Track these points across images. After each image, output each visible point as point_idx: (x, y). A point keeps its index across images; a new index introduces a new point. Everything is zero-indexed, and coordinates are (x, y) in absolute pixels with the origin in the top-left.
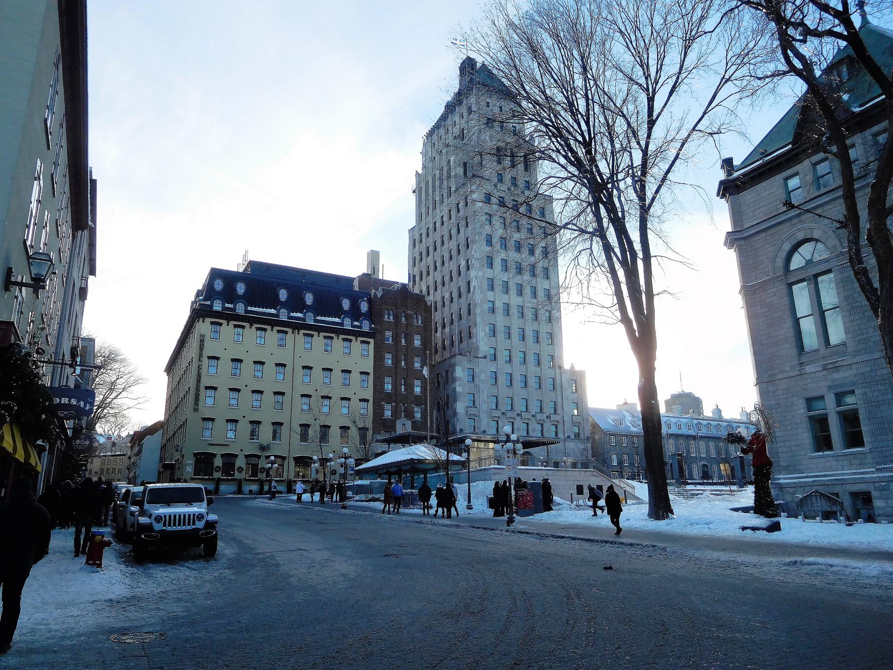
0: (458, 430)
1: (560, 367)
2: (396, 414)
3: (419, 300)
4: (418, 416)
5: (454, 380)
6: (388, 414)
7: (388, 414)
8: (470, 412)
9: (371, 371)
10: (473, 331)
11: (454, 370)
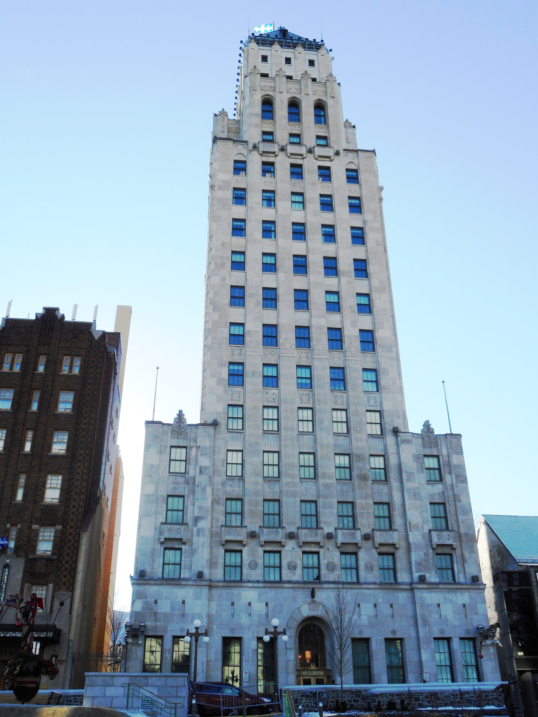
4: (45, 547)
8: (167, 535)
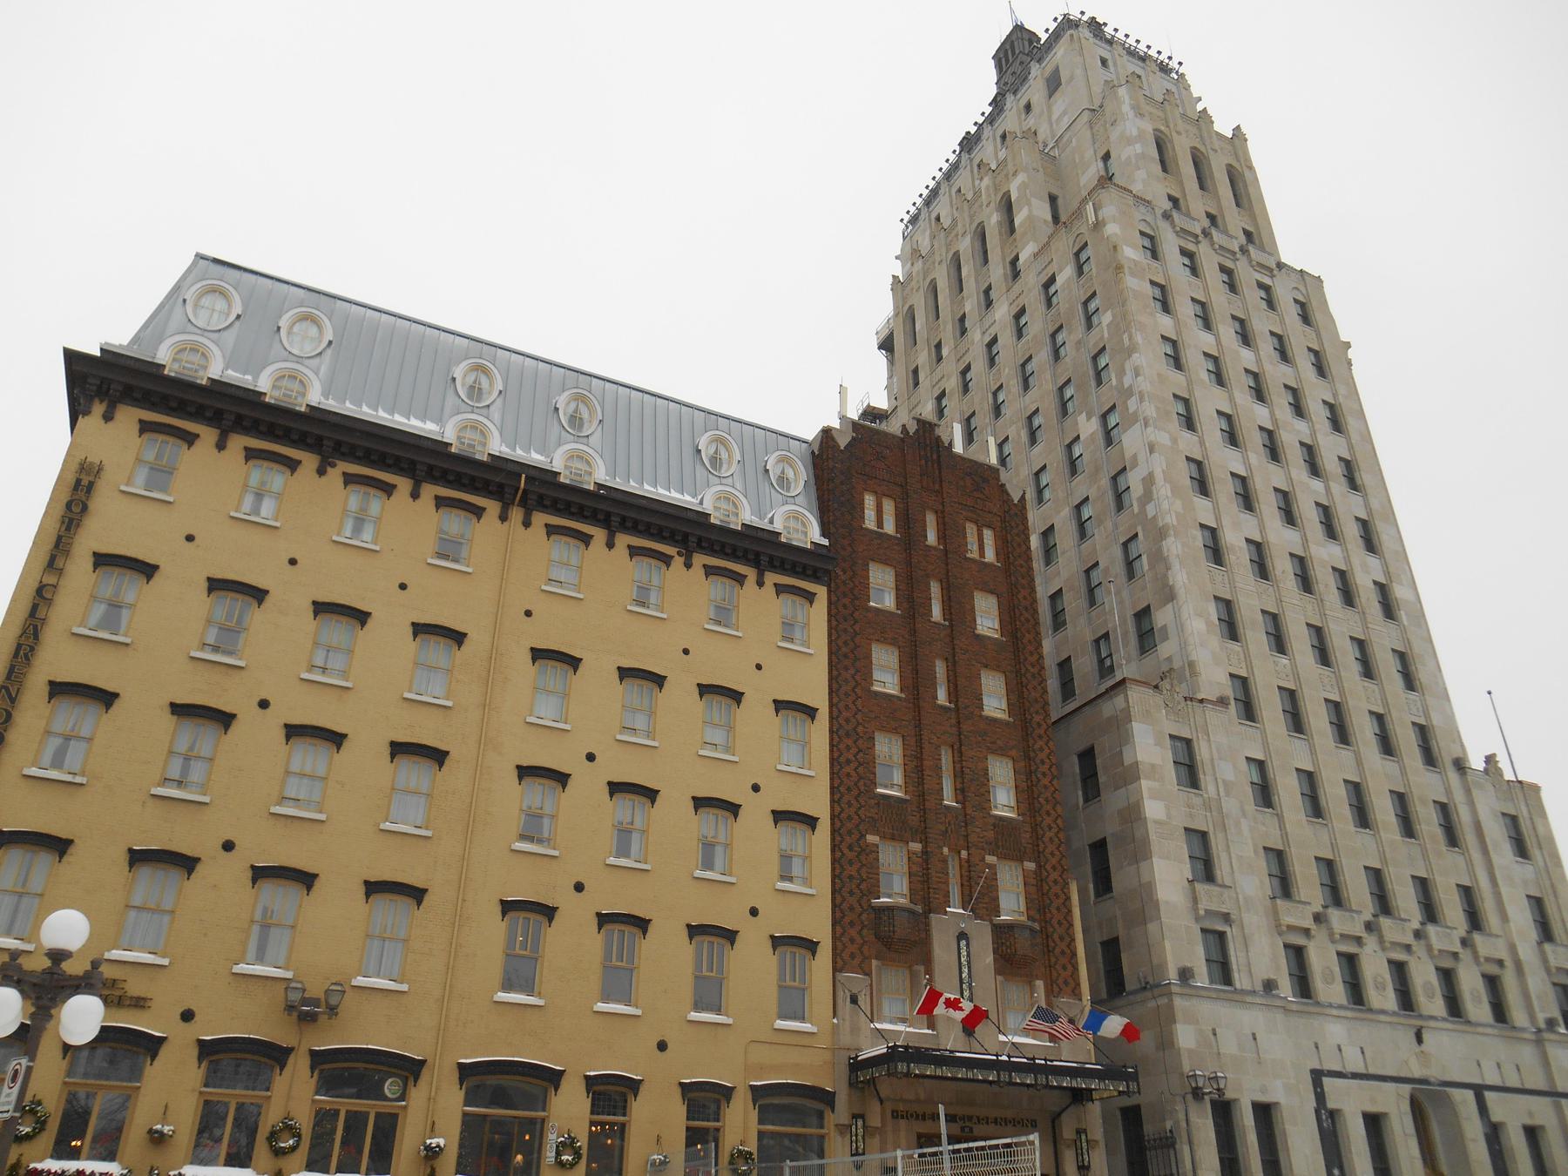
0: (1173, 975)
1: (1460, 765)
2: (927, 893)
3: (981, 482)
4: (1012, 906)
5: (1131, 775)
6: (895, 891)
7: (895, 891)
9: (818, 697)
10: (1161, 617)
11: (1125, 738)
